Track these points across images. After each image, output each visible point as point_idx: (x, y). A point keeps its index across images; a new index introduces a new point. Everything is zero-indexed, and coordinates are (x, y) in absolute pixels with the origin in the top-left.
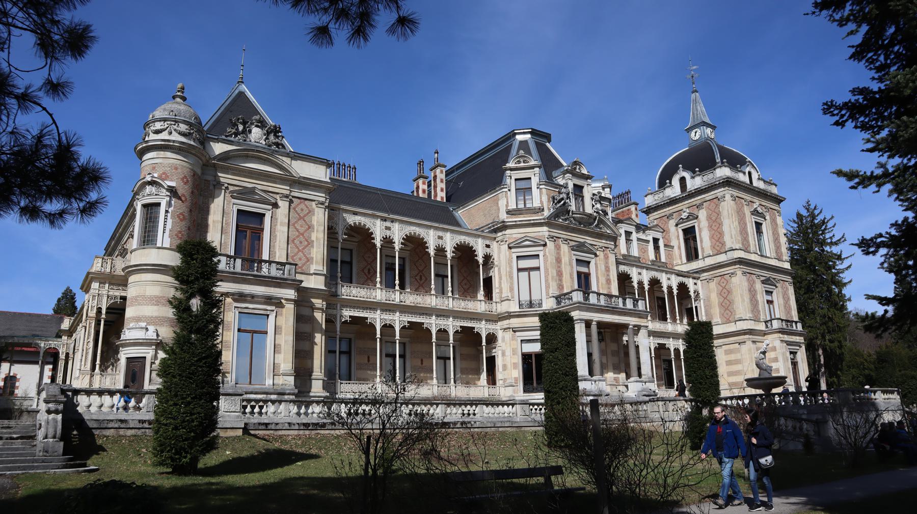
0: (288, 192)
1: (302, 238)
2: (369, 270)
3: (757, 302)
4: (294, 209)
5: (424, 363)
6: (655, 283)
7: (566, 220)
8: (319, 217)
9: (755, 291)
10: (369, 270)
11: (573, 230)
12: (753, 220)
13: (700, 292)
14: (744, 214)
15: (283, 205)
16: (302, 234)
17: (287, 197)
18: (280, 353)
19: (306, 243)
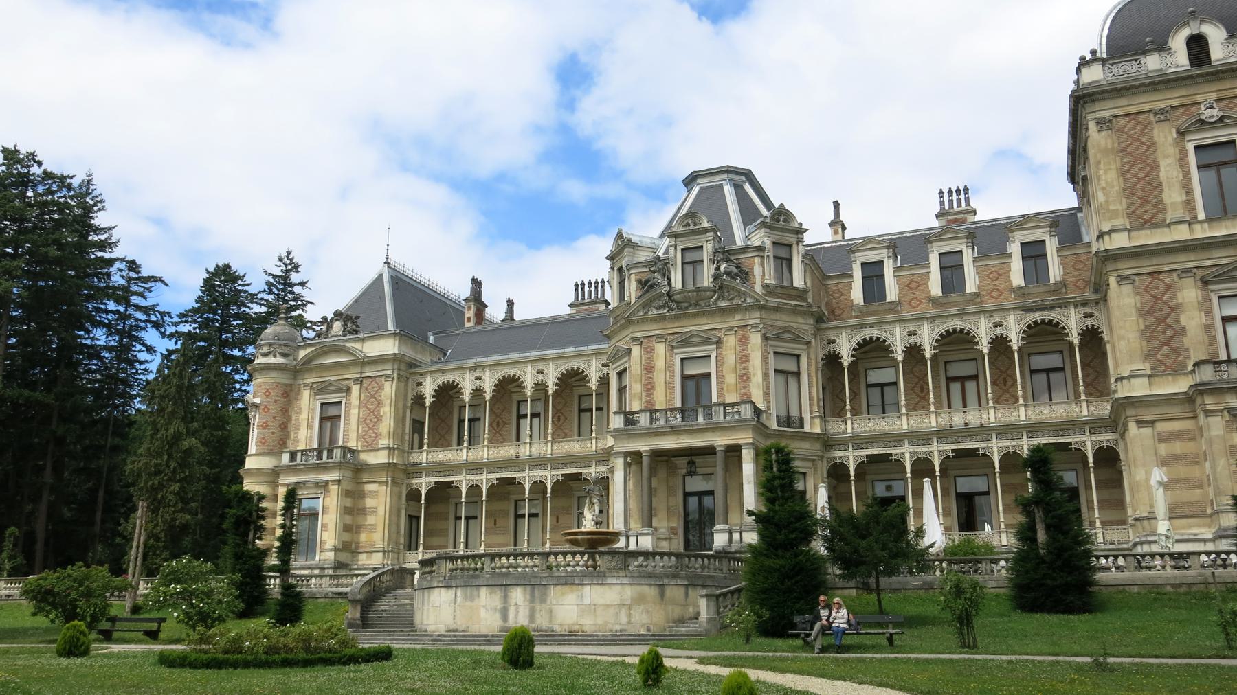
0: (358, 375)
1: (372, 416)
2: (498, 423)
3: (1179, 331)
4: (366, 389)
5: (560, 520)
6: (955, 342)
7: (662, 307)
8: (389, 390)
9: (1175, 309)
10: (498, 423)
11: (675, 317)
12: (1190, 148)
13: (1104, 328)
14: (1152, 146)
15: (355, 389)
16: (372, 412)
17: (356, 380)
18: (326, 531)
19: (376, 420)
